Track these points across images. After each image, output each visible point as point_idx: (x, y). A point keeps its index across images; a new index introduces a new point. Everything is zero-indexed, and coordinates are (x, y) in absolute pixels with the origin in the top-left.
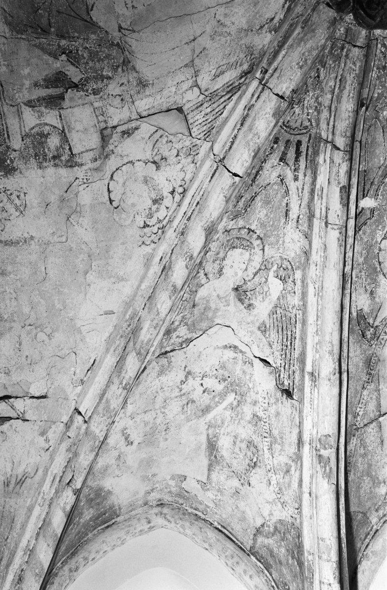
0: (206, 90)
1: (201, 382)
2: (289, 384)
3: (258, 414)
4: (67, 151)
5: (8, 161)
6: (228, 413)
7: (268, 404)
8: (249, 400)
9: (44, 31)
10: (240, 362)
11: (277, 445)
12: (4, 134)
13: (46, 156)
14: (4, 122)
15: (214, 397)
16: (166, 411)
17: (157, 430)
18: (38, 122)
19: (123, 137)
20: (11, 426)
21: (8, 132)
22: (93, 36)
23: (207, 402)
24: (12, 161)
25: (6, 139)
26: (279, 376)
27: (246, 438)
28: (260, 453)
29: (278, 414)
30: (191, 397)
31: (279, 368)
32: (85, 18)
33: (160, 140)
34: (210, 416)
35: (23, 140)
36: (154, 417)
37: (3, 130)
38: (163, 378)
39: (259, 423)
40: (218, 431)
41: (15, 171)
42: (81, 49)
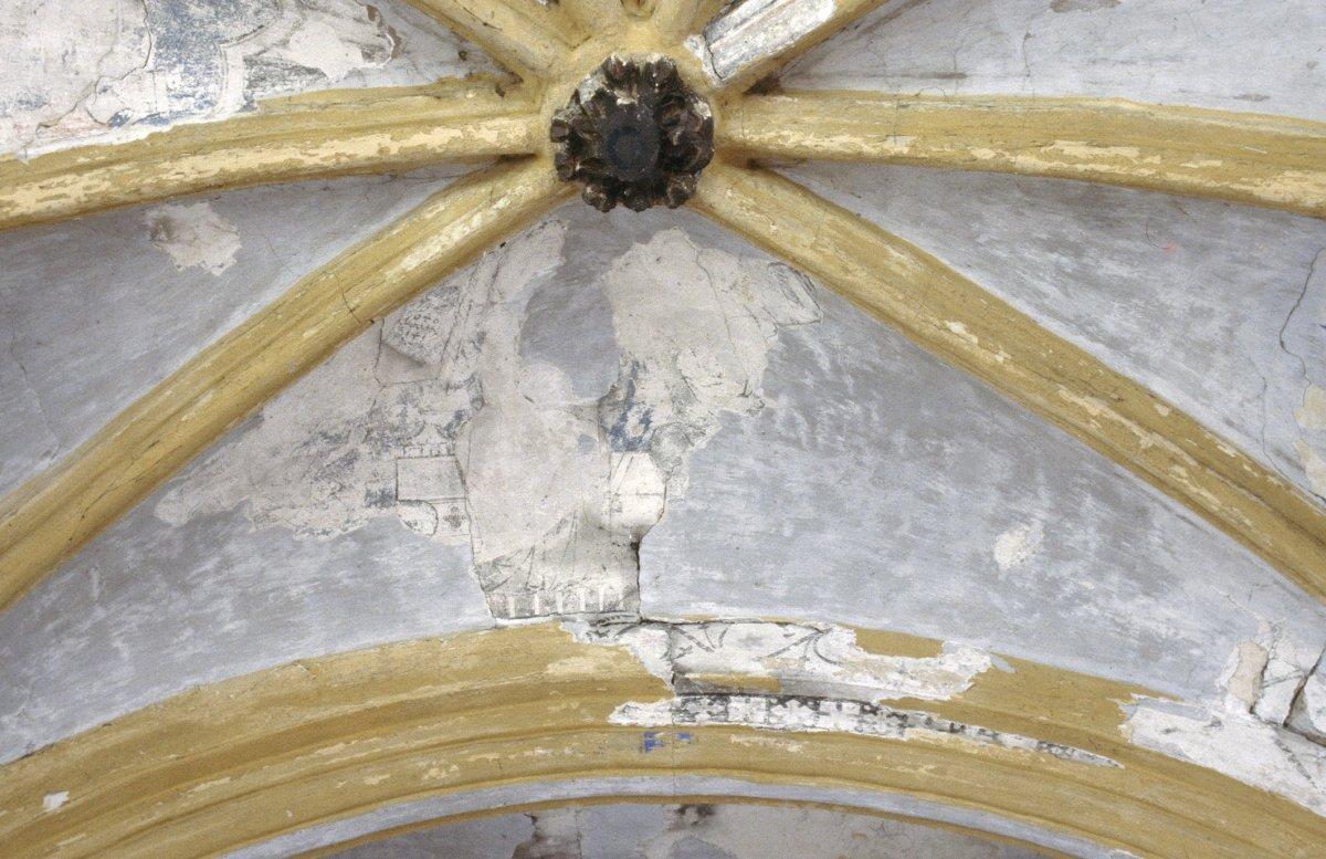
0: (817, 314)
20: (1314, 694)
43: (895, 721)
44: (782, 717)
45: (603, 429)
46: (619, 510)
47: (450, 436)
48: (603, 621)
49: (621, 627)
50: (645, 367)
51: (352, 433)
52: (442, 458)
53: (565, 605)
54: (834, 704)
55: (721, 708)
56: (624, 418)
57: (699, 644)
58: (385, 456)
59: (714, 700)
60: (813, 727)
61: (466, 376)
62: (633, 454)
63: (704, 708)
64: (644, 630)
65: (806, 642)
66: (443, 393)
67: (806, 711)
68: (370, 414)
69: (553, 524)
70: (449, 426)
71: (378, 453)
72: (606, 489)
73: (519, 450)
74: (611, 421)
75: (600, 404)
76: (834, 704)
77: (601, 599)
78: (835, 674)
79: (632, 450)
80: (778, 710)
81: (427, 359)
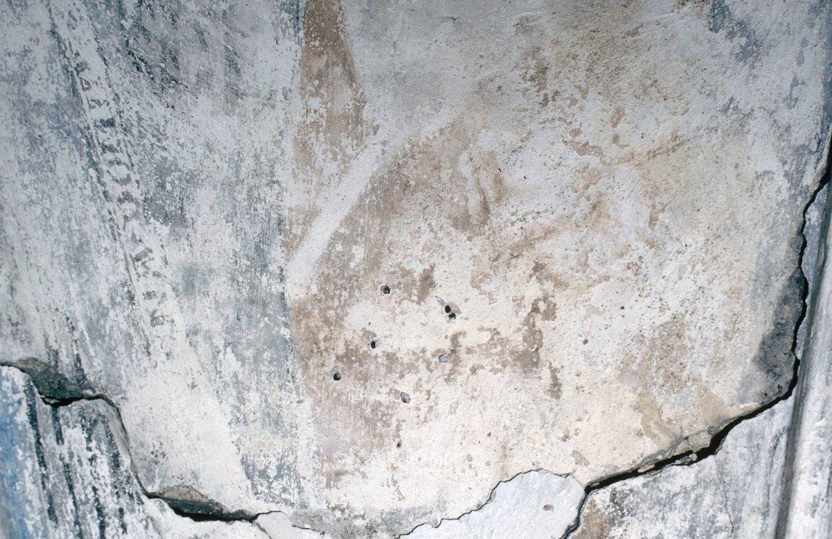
1: (457, 325)
2: (59, 438)
3: (165, 230)
6: (293, 198)
7: (132, 298)
8: (220, 287)
10: (305, 468)
11: (50, 100)
15: (374, 263)
16: (574, 159)
17: (583, 63)
23: (399, 233)
26: (115, 463)
27: (188, 97)
28: (114, 41)
29: (78, 259)
30: (478, 241)
31: (124, 501)
34: (366, 166)
36: (622, 127)
38: (644, 316)
39: (153, 184)
40: (315, 103)
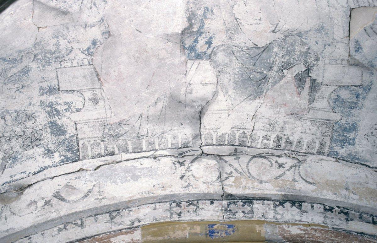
4: (356, 88)
5: (347, 126)
9: (265, 78)
12: (326, 123)
13: (353, 102)
14: (318, 120)
18: (326, 100)
19: (361, 53)
21: (326, 120)
22: (276, 49)
24: (348, 124)
25: (330, 122)
32: (262, 51)
33: (374, 29)
35: (336, 112)
37: (323, 122)
41: (356, 124)
42: (282, 60)
43: (343, 217)
44: (283, 214)
45: (183, 48)
46: (191, 93)
47: (89, 54)
48: (181, 154)
49: (192, 158)
50: (212, 11)
51: (24, 57)
52: (85, 67)
53: (160, 144)
54: (310, 205)
55: (249, 208)
56: (196, 41)
57: (235, 170)
58: (48, 68)
59: (245, 203)
60: (300, 221)
61: (98, 18)
62: (201, 61)
63: (240, 208)
64: (205, 160)
65: (293, 169)
66: (83, 30)
67: (295, 210)
68: (34, 46)
69: (153, 100)
70: (88, 49)
71: (44, 67)
72: (184, 81)
73: (133, 61)
74: (189, 42)
75: (183, 33)
76: (310, 205)
77: (180, 142)
78: (313, 191)
79: (200, 59)
80: (280, 209)
81: (70, 10)
